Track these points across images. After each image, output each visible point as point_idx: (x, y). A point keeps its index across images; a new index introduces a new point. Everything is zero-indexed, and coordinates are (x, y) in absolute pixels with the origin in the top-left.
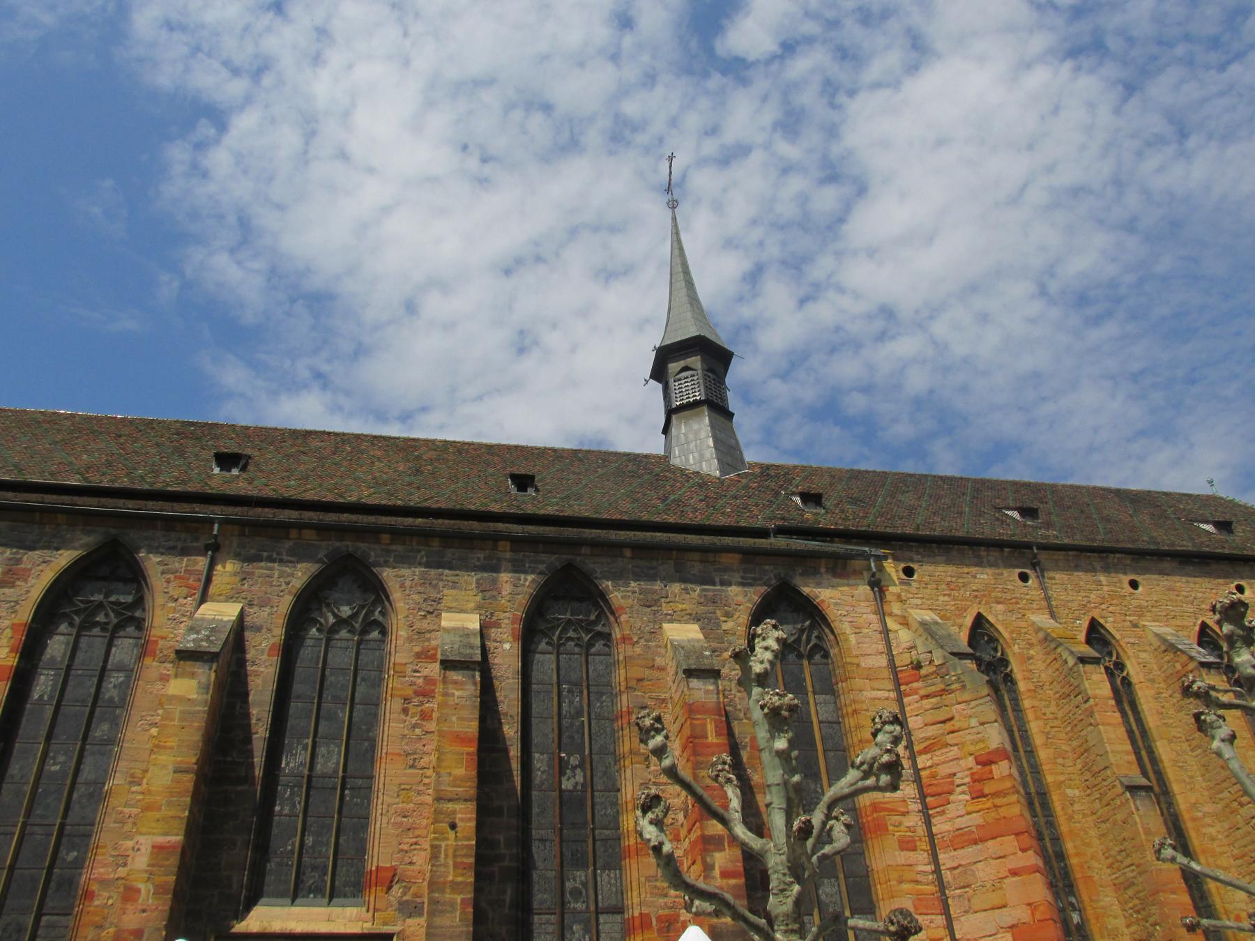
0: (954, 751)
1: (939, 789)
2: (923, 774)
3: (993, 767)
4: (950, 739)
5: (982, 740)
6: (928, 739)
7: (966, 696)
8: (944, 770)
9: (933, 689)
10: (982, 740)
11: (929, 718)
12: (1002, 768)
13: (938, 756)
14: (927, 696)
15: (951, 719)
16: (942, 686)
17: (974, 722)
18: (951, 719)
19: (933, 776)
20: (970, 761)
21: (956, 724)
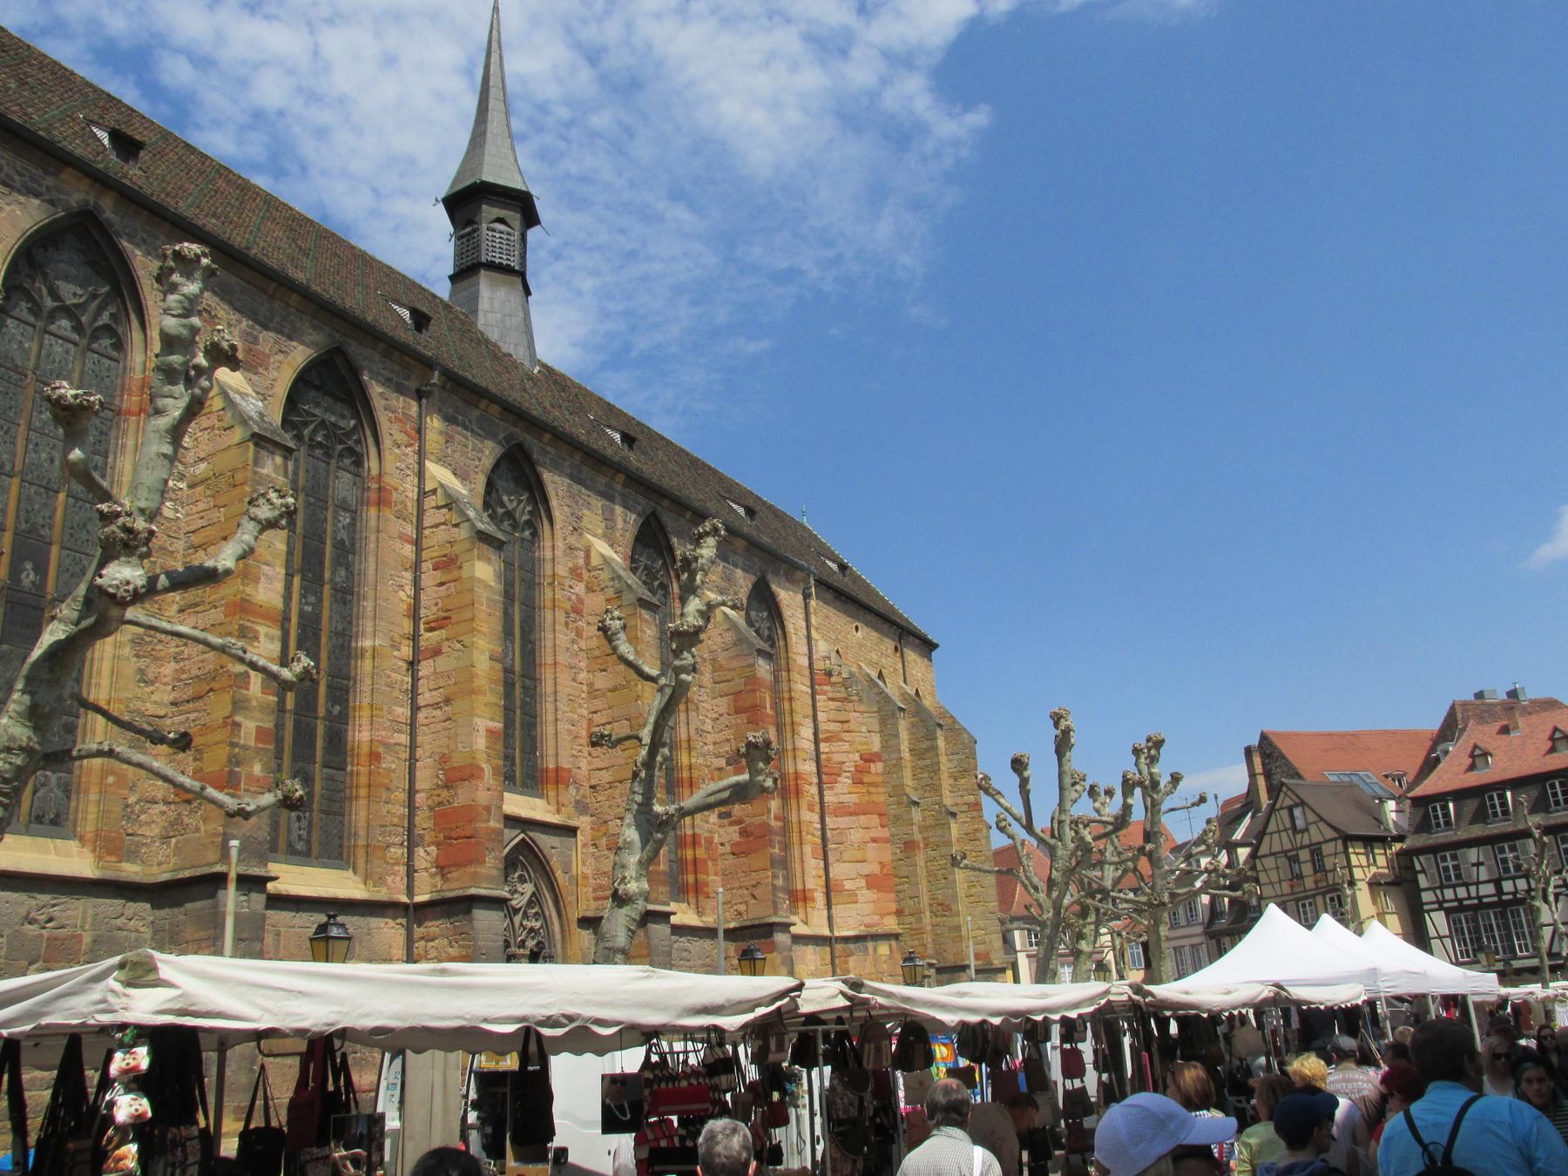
0: (846, 747)
1: (831, 771)
2: (823, 756)
3: (872, 765)
4: (845, 736)
5: (867, 744)
6: (829, 731)
7: (862, 708)
8: (836, 758)
9: (838, 695)
10: (867, 744)
11: (832, 717)
12: (877, 767)
13: (835, 746)
14: (833, 699)
15: (847, 722)
16: (845, 695)
17: (864, 729)
18: (847, 722)
19: (829, 760)
20: (857, 757)
21: (852, 726)
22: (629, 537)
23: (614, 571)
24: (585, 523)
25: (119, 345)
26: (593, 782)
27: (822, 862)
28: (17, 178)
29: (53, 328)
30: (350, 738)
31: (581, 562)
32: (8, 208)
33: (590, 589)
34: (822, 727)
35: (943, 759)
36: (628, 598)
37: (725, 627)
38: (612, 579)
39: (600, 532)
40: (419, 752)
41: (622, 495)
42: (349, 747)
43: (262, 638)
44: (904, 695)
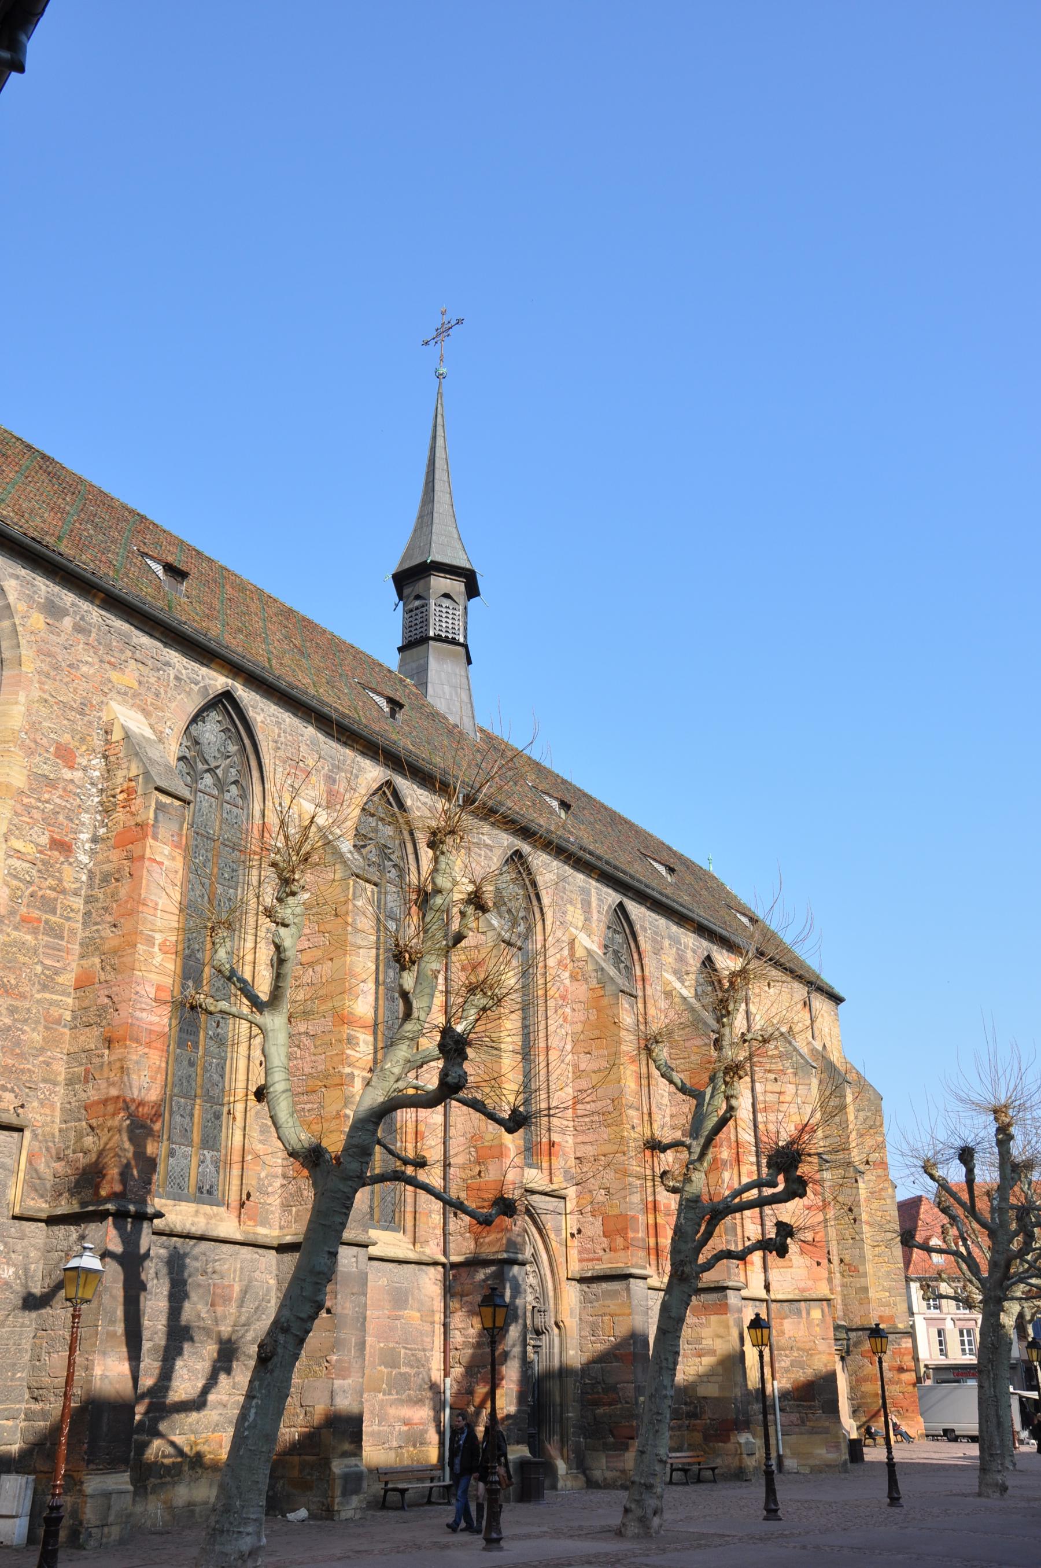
22: (603, 926)
23: (597, 962)
24: (569, 918)
25: (244, 796)
26: (578, 1155)
27: (759, 1227)
28: (184, 671)
29: (201, 786)
30: (399, 1118)
31: (566, 952)
32: (179, 697)
33: (573, 978)
34: (760, 1097)
35: (851, 1117)
36: (610, 989)
37: (684, 1007)
38: (596, 971)
39: (580, 925)
40: (452, 1132)
41: (596, 888)
42: (398, 1126)
43: (361, 1043)
44: (813, 1050)
